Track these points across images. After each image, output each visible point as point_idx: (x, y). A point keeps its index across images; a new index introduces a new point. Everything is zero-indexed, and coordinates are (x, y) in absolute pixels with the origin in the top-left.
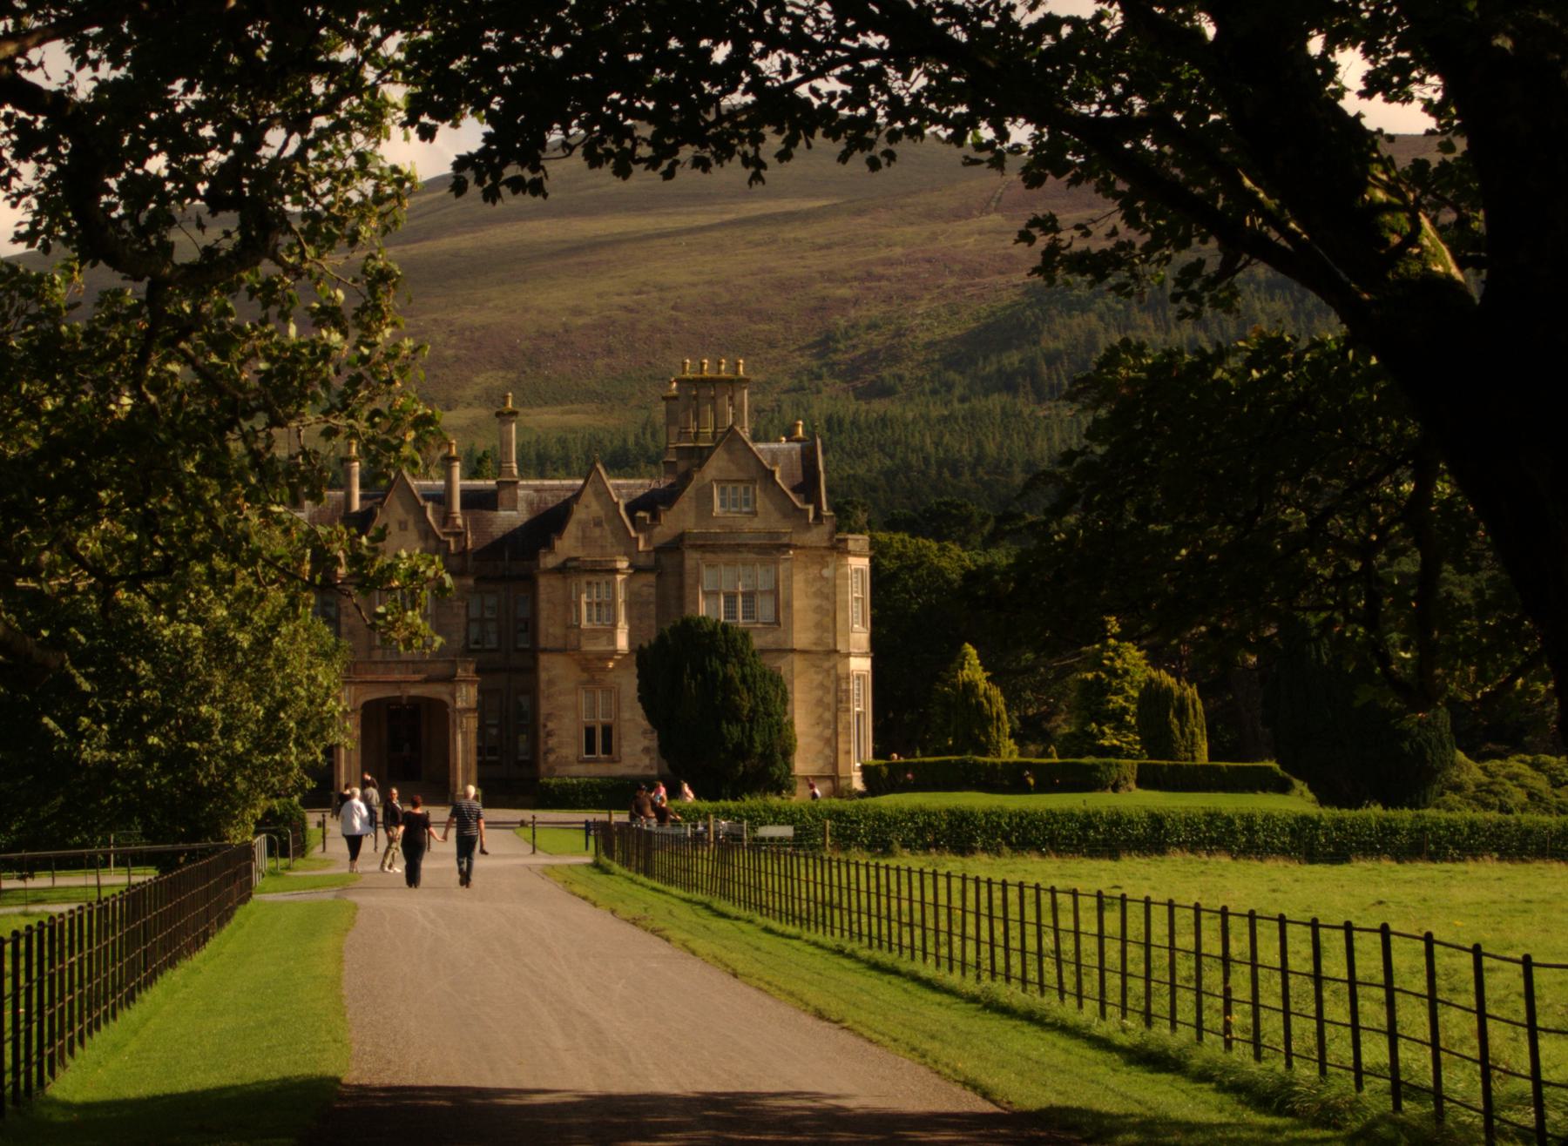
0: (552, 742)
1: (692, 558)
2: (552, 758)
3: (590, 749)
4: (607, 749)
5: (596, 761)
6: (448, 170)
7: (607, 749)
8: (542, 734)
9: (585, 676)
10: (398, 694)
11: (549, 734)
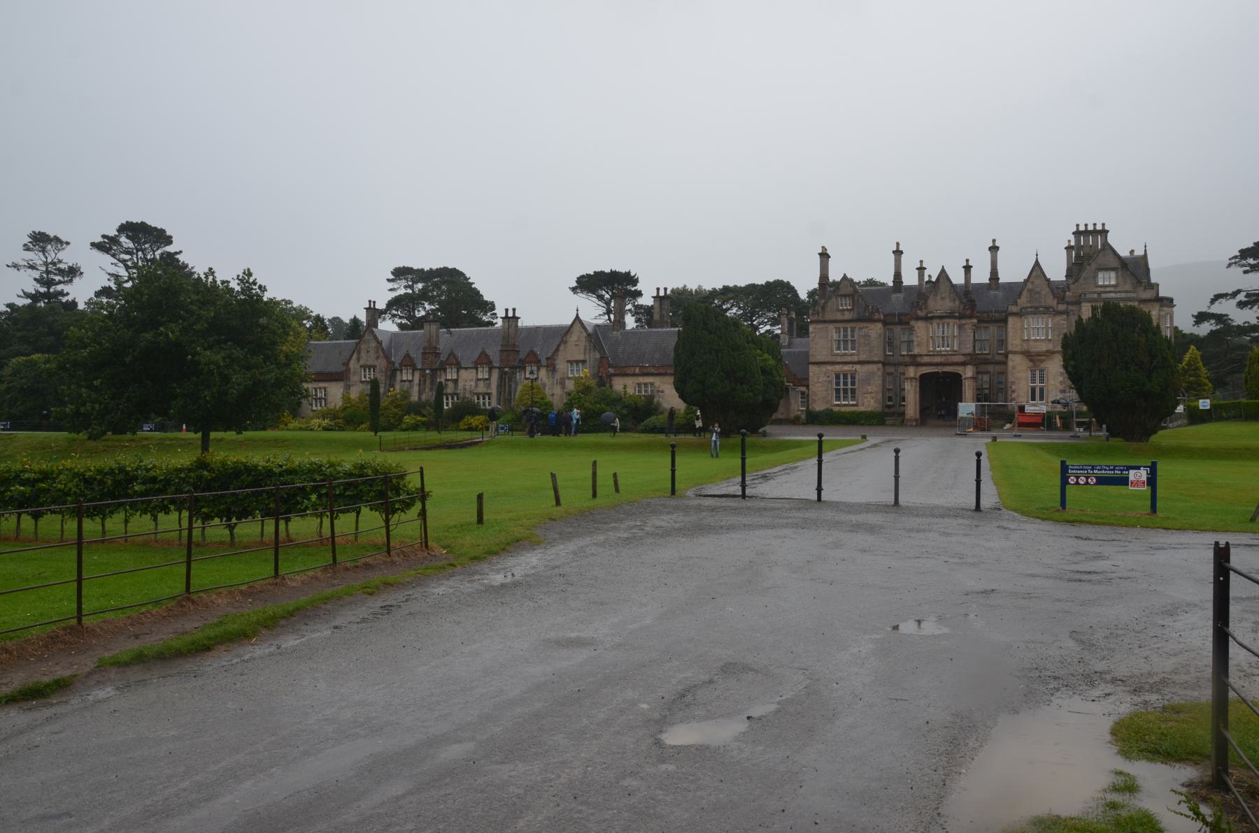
4: (1042, 398)
11: (1013, 391)
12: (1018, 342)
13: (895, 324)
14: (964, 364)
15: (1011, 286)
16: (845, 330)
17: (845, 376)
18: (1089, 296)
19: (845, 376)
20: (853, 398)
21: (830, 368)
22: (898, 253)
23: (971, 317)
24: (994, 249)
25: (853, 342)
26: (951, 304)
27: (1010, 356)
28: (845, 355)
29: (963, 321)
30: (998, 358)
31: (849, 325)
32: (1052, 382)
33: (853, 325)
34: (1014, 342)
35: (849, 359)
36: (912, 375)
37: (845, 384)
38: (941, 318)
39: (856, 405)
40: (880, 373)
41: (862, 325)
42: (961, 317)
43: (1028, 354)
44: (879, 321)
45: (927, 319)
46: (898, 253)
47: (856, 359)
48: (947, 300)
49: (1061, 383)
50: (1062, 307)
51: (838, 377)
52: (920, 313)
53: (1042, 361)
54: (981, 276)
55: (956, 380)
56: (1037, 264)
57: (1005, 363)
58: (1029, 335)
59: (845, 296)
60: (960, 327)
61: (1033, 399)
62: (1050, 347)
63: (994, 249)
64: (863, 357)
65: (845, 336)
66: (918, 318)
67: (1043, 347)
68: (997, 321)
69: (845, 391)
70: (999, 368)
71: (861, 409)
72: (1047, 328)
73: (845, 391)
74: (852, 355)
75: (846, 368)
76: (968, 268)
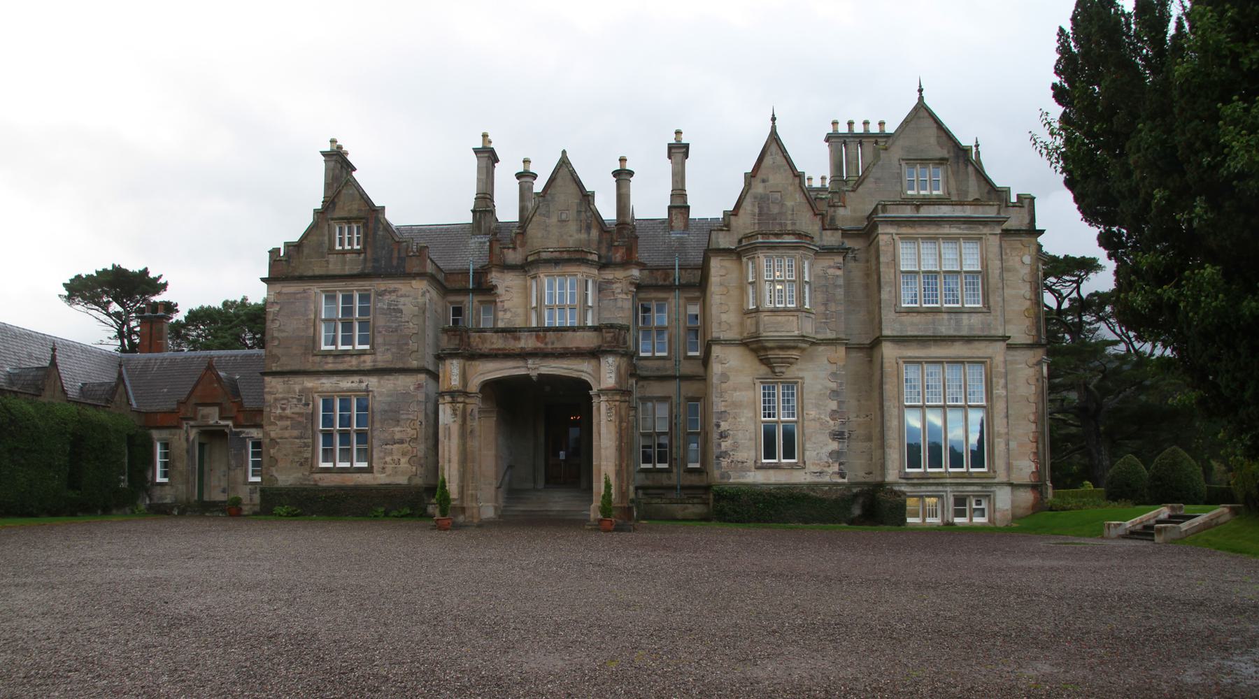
0: (725, 445)
1: (885, 234)
2: (725, 462)
3: (770, 453)
4: (789, 453)
5: (776, 467)
6: (721, 216)
7: (789, 453)
8: (715, 436)
9: (763, 370)
10: (523, 372)
11: (723, 436)
12: (731, 317)
13: (465, 291)
14: (594, 354)
15: (710, 227)
16: (348, 299)
17: (345, 406)
18: (893, 213)
19: (345, 406)
20: (365, 454)
21: (310, 383)
22: (487, 156)
23: (625, 264)
24: (679, 151)
25: (364, 325)
26: (584, 236)
27: (716, 350)
28: (345, 354)
29: (609, 275)
30: (687, 368)
31: (356, 288)
32: (812, 413)
33: (366, 285)
34: (724, 316)
35: (353, 363)
36: (455, 382)
37: (345, 421)
38: (556, 262)
39: (369, 470)
40: (421, 397)
41: (381, 285)
42: (603, 265)
43: (756, 346)
44: (421, 275)
45: (524, 268)
46: (487, 156)
47: (368, 362)
48: (573, 227)
49: (833, 414)
50: (831, 239)
51: (328, 405)
52: (513, 257)
53: (789, 362)
54: (650, 203)
55: (575, 398)
56: (774, 137)
57: (702, 378)
58: (758, 297)
59: (349, 220)
60: (601, 288)
61: (770, 453)
62: (809, 328)
63: (679, 151)
64: (383, 359)
65: (348, 311)
66: (506, 267)
67: (791, 328)
68: (683, 287)
69: (345, 436)
70: (690, 389)
71: (379, 478)
72: (800, 283)
73: (345, 436)
74: (363, 353)
75: (346, 383)
76: (623, 175)
